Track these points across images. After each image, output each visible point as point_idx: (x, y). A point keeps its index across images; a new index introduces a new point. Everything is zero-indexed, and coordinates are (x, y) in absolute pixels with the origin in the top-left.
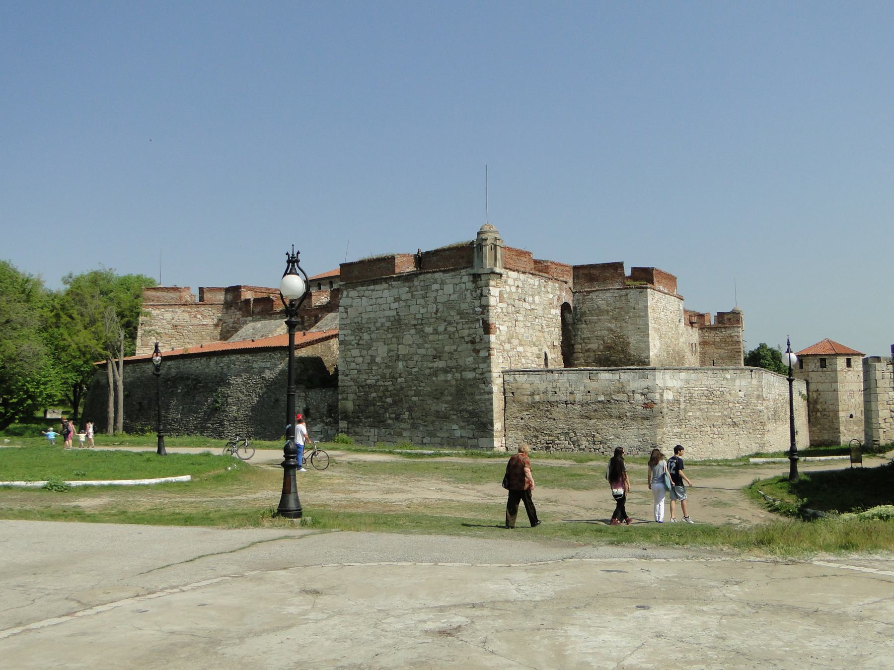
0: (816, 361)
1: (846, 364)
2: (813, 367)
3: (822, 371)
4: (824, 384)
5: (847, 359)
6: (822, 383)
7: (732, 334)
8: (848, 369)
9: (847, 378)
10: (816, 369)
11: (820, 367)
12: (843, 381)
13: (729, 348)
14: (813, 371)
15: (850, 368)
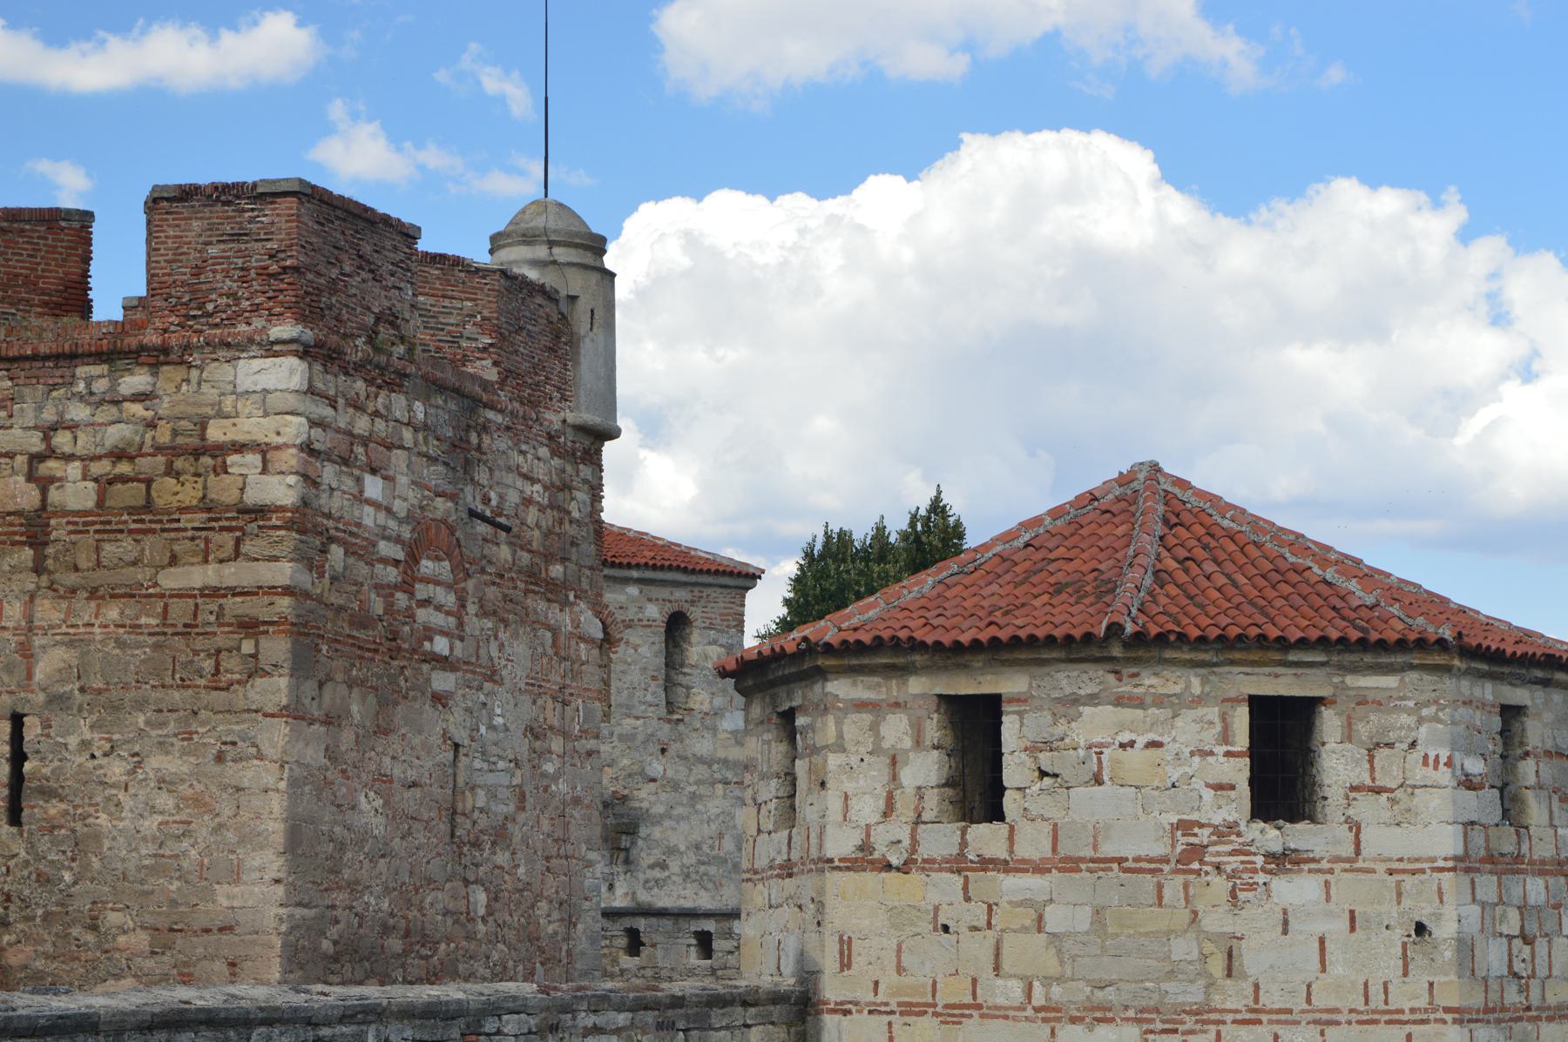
0: (896, 729)
1: (1239, 770)
2: (867, 809)
3: (957, 864)
4: (972, 1024)
5: (1259, 705)
6: (954, 1014)
7: (215, 433)
8: (1270, 836)
9: (1252, 961)
10: (890, 837)
11: (932, 802)
12: (1193, 995)
13: (171, 580)
14: (865, 860)
15: (1299, 835)
